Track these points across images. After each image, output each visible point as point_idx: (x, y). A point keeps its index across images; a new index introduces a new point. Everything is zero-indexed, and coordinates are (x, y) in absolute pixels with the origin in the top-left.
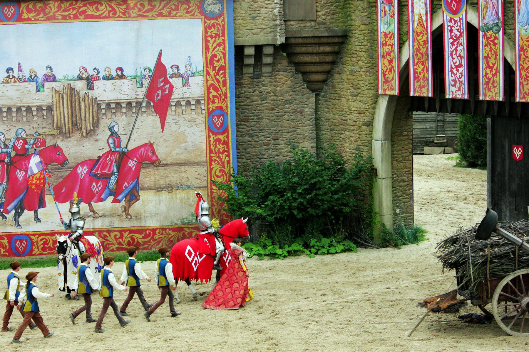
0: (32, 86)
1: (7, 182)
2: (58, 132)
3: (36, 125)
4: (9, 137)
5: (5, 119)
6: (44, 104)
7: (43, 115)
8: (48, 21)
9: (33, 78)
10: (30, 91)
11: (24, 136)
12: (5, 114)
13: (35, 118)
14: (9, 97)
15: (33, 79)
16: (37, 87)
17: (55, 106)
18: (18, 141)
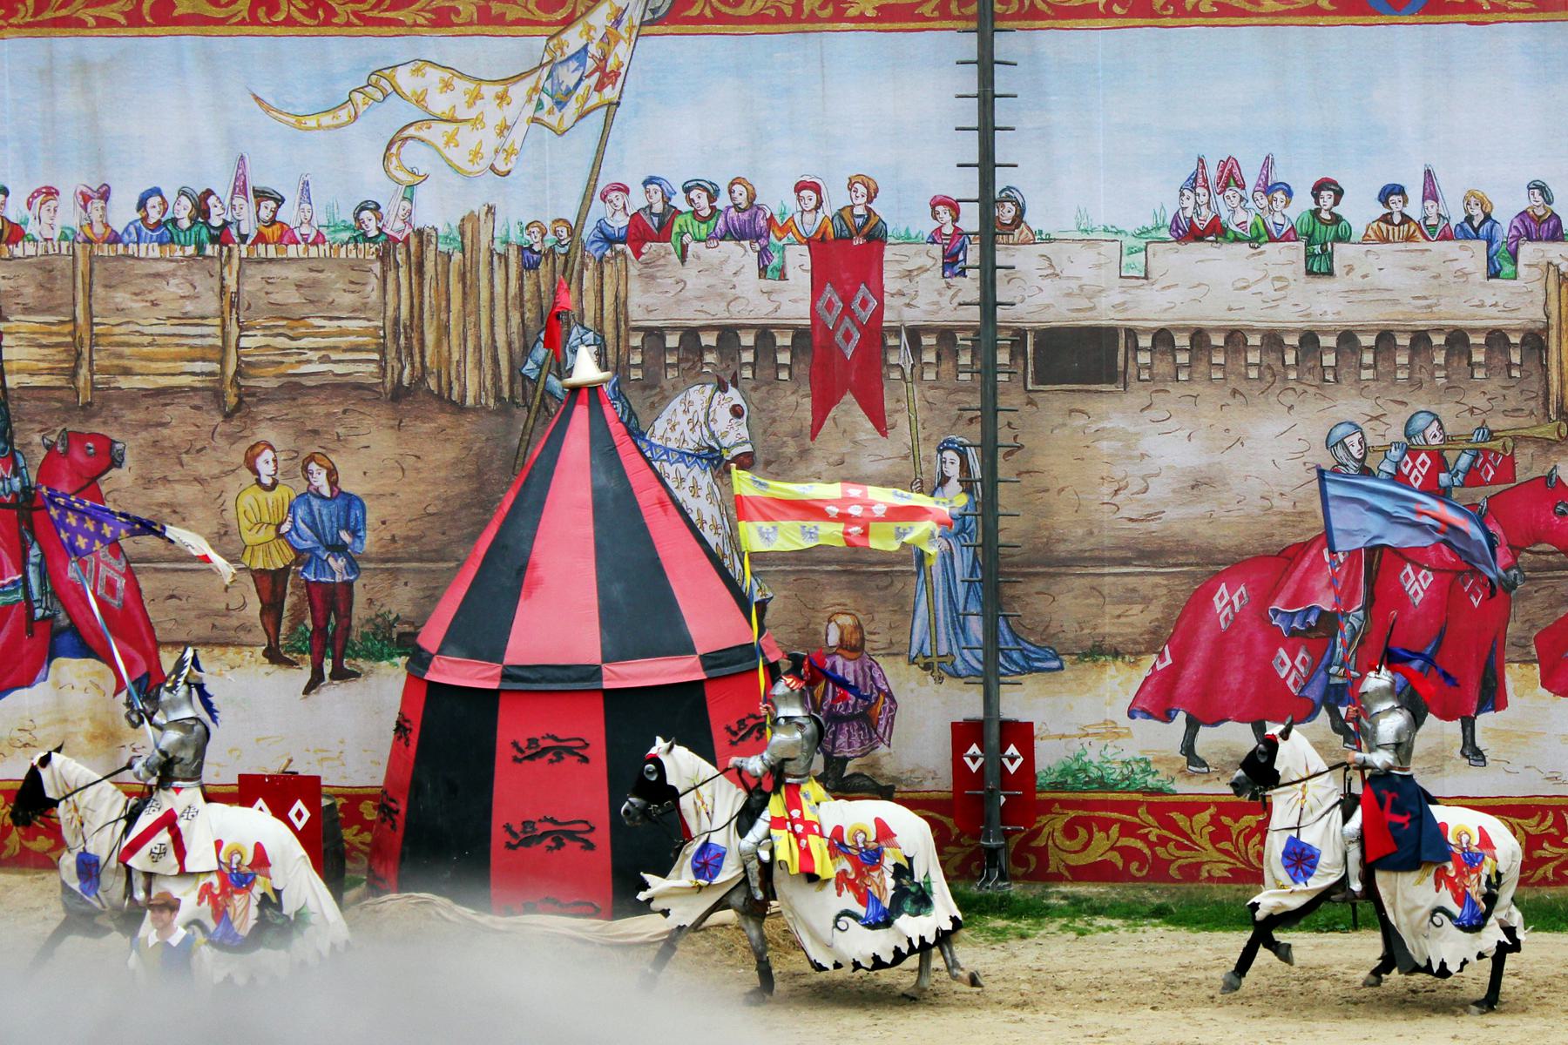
0: (1473, 256)
1: (1364, 608)
2: (1563, 431)
3: (1481, 402)
4: (1381, 442)
5: (1367, 374)
6: (1514, 323)
7: (1510, 365)
8: (1542, 16)
9: (1476, 227)
10: (1465, 274)
11: (1435, 442)
12: (1368, 358)
13: (1479, 374)
14: (1386, 296)
15: (1476, 230)
16: (1489, 259)
17: (1553, 333)
18: (1414, 459)
